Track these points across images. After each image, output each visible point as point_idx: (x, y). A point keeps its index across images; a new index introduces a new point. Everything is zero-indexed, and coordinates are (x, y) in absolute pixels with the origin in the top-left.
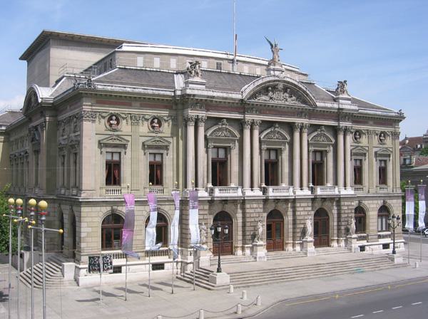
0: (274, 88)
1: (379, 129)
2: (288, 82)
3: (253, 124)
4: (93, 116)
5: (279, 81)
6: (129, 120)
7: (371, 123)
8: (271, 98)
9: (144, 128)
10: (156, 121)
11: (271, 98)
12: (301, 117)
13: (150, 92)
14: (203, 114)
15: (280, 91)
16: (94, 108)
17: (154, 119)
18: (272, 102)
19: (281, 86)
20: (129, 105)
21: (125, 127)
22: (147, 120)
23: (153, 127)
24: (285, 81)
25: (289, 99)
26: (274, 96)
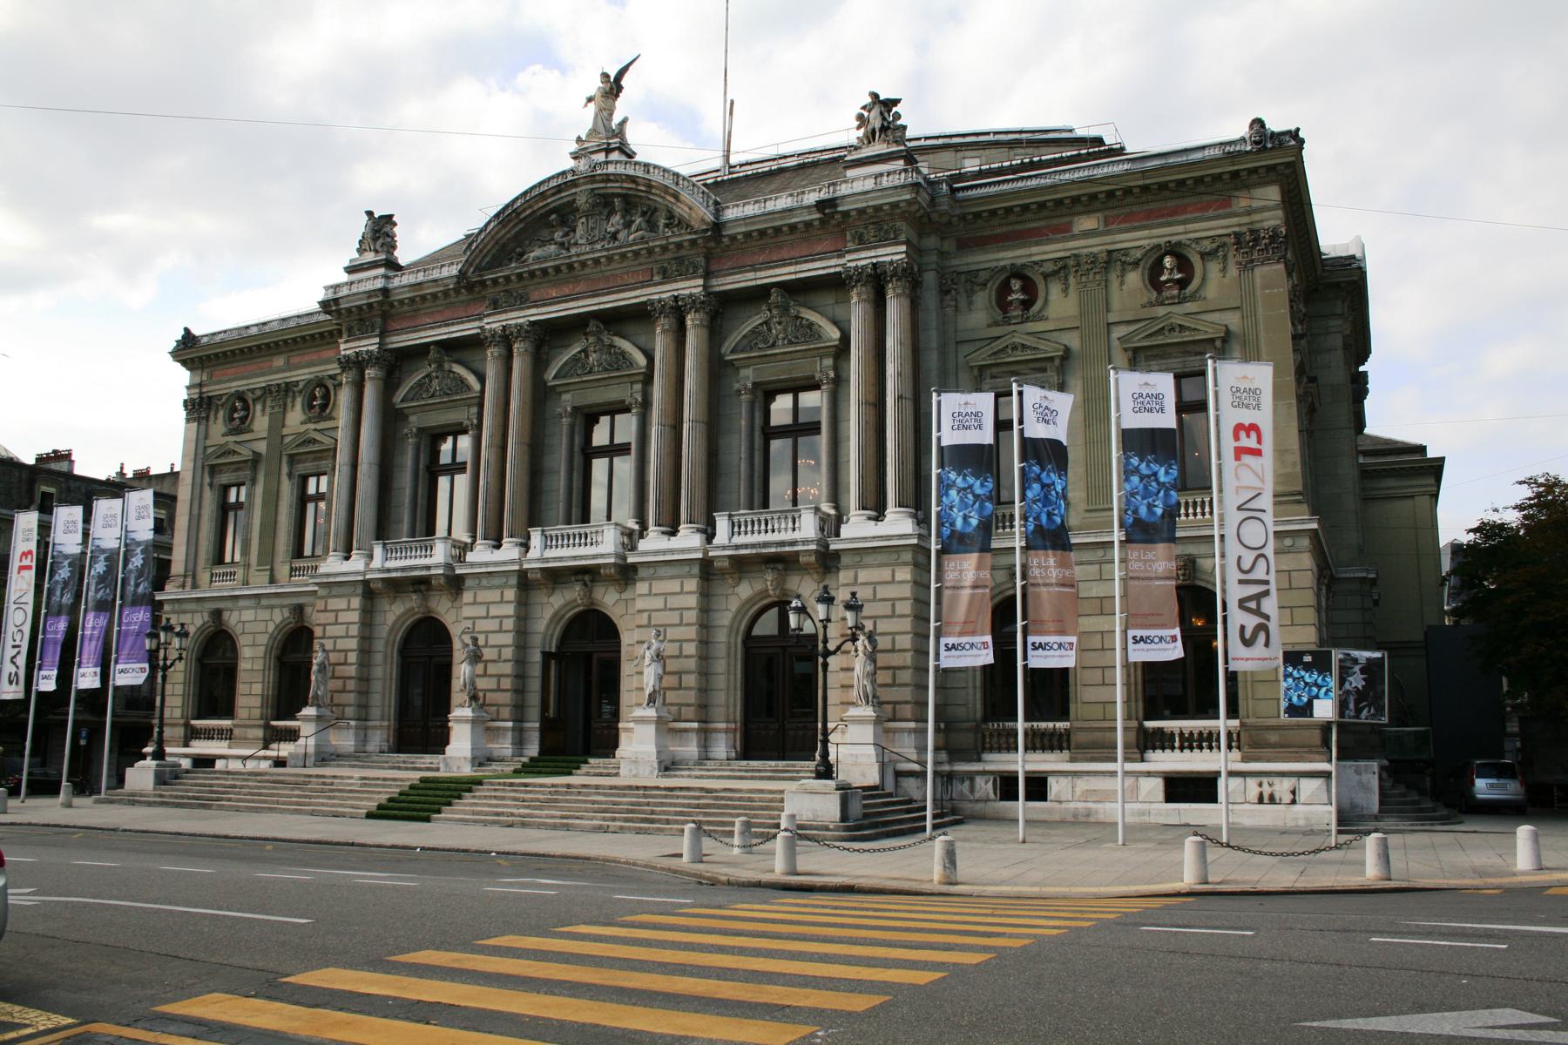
1: (1138, 239)
2: (607, 178)
3: (506, 339)
5: (574, 184)
7: (1087, 223)
9: (295, 417)
10: (318, 393)
12: (667, 277)
14: (370, 344)
17: (315, 389)
19: (582, 201)
21: (261, 423)
23: (311, 407)
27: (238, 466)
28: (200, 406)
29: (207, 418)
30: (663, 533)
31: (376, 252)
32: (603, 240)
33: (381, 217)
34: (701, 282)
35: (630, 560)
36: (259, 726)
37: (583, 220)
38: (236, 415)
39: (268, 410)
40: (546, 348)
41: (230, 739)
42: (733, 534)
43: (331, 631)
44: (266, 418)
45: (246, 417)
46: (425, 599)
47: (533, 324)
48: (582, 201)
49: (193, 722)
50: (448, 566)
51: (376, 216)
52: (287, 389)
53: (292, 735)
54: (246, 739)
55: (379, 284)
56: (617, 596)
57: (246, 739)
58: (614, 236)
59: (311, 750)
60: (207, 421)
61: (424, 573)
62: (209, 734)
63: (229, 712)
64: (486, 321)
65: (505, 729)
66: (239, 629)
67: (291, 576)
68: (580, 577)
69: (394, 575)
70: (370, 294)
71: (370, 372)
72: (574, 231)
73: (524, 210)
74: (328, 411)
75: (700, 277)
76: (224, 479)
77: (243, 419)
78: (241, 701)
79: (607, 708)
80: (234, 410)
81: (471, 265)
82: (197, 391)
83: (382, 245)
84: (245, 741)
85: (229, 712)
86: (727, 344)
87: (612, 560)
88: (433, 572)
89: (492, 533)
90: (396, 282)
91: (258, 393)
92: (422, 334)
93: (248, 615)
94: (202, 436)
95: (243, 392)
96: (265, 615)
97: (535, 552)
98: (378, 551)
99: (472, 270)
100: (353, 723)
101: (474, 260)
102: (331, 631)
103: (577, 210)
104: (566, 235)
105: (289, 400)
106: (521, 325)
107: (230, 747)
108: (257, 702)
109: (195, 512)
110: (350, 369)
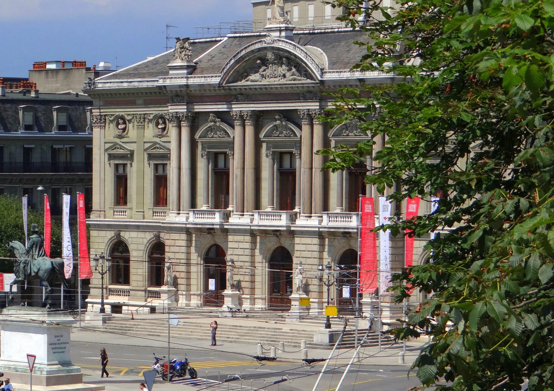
0: (265, 62)
2: (279, 49)
3: (242, 118)
4: (102, 120)
5: (265, 48)
6: (136, 123)
8: (263, 76)
9: (150, 132)
11: (263, 75)
13: (145, 85)
14: (182, 109)
15: (273, 63)
16: (102, 111)
18: (265, 82)
20: (131, 103)
21: (132, 132)
22: (150, 121)
24: (273, 48)
25: (288, 74)
26: (268, 72)
27: (123, 157)
28: (101, 119)
29: (105, 126)
30: (306, 216)
31: (182, 60)
32: (279, 76)
33: (183, 40)
34: (318, 104)
35: (292, 229)
36: (142, 291)
37: (271, 65)
38: (120, 127)
39: (135, 127)
40: (261, 119)
41: (129, 296)
42: (329, 221)
43: (173, 249)
44: (135, 131)
45: (126, 127)
46: (213, 236)
47: (252, 111)
48: (270, 56)
49: (110, 287)
50: (221, 225)
51: (181, 39)
52: (144, 117)
53: (157, 295)
54: (136, 296)
55: (183, 82)
56: (290, 242)
57: (136, 296)
58: (284, 76)
59: (166, 306)
60: (105, 128)
61: (211, 227)
62: (118, 293)
63: (127, 281)
64: (233, 106)
65: (247, 299)
66: (130, 240)
67: (153, 216)
68: (275, 233)
69: (198, 226)
70: (180, 86)
71: (183, 124)
72: (268, 68)
73: (246, 57)
74: (165, 132)
75: (318, 102)
76: (117, 162)
77: (124, 130)
78: (132, 277)
79: (289, 290)
80: (118, 124)
81: (224, 80)
82: (98, 111)
83: (185, 55)
84: (136, 298)
85: (127, 281)
86: (330, 133)
87: (285, 229)
88: (215, 227)
89: (240, 209)
90: (192, 81)
91: (129, 118)
92: (206, 107)
93: (134, 234)
94: (102, 136)
95: (122, 116)
96: (141, 235)
97: (255, 222)
98: (191, 214)
99: (225, 82)
100: (184, 293)
101: (225, 78)
102: (173, 249)
103: (268, 60)
104: (264, 70)
105: (146, 123)
106: (247, 111)
107: (129, 300)
108: (140, 278)
109: (102, 177)
110: (174, 121)
